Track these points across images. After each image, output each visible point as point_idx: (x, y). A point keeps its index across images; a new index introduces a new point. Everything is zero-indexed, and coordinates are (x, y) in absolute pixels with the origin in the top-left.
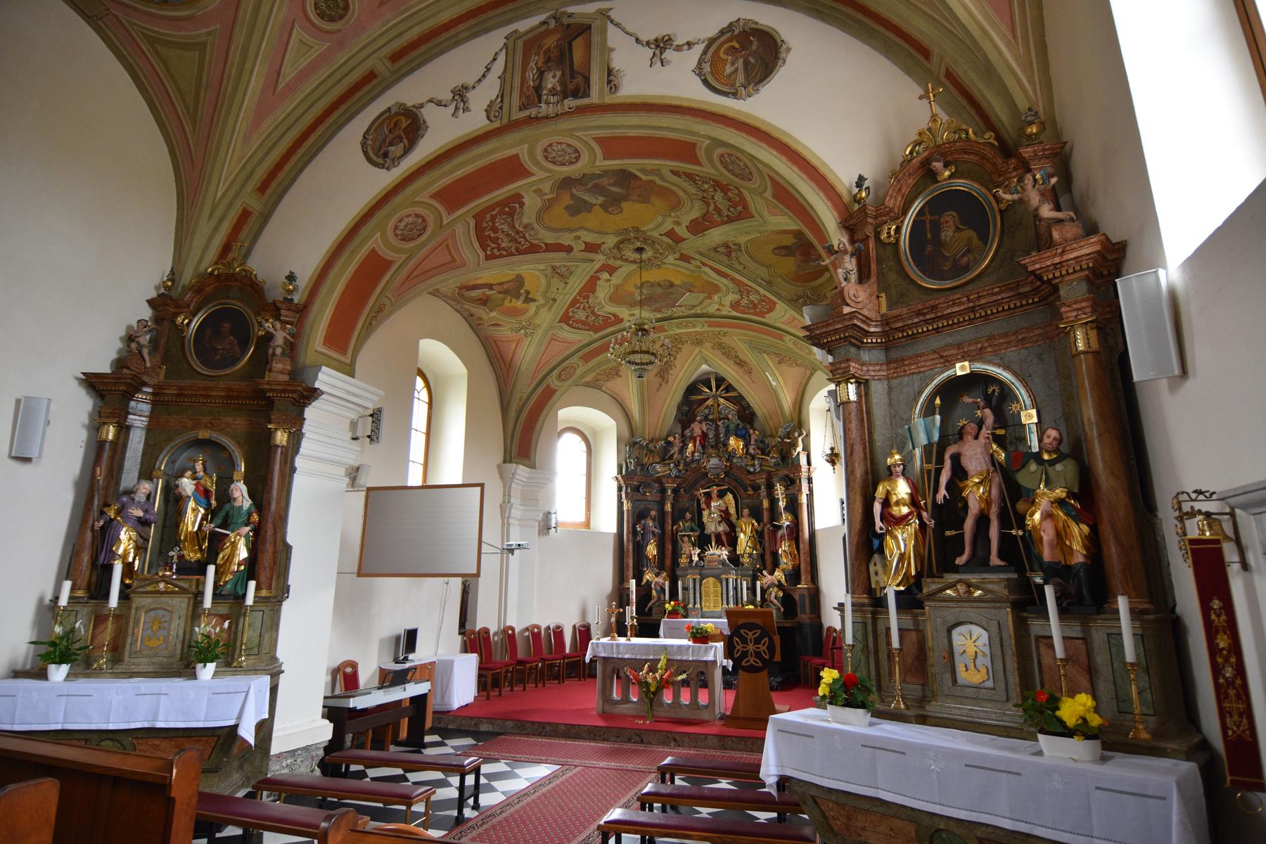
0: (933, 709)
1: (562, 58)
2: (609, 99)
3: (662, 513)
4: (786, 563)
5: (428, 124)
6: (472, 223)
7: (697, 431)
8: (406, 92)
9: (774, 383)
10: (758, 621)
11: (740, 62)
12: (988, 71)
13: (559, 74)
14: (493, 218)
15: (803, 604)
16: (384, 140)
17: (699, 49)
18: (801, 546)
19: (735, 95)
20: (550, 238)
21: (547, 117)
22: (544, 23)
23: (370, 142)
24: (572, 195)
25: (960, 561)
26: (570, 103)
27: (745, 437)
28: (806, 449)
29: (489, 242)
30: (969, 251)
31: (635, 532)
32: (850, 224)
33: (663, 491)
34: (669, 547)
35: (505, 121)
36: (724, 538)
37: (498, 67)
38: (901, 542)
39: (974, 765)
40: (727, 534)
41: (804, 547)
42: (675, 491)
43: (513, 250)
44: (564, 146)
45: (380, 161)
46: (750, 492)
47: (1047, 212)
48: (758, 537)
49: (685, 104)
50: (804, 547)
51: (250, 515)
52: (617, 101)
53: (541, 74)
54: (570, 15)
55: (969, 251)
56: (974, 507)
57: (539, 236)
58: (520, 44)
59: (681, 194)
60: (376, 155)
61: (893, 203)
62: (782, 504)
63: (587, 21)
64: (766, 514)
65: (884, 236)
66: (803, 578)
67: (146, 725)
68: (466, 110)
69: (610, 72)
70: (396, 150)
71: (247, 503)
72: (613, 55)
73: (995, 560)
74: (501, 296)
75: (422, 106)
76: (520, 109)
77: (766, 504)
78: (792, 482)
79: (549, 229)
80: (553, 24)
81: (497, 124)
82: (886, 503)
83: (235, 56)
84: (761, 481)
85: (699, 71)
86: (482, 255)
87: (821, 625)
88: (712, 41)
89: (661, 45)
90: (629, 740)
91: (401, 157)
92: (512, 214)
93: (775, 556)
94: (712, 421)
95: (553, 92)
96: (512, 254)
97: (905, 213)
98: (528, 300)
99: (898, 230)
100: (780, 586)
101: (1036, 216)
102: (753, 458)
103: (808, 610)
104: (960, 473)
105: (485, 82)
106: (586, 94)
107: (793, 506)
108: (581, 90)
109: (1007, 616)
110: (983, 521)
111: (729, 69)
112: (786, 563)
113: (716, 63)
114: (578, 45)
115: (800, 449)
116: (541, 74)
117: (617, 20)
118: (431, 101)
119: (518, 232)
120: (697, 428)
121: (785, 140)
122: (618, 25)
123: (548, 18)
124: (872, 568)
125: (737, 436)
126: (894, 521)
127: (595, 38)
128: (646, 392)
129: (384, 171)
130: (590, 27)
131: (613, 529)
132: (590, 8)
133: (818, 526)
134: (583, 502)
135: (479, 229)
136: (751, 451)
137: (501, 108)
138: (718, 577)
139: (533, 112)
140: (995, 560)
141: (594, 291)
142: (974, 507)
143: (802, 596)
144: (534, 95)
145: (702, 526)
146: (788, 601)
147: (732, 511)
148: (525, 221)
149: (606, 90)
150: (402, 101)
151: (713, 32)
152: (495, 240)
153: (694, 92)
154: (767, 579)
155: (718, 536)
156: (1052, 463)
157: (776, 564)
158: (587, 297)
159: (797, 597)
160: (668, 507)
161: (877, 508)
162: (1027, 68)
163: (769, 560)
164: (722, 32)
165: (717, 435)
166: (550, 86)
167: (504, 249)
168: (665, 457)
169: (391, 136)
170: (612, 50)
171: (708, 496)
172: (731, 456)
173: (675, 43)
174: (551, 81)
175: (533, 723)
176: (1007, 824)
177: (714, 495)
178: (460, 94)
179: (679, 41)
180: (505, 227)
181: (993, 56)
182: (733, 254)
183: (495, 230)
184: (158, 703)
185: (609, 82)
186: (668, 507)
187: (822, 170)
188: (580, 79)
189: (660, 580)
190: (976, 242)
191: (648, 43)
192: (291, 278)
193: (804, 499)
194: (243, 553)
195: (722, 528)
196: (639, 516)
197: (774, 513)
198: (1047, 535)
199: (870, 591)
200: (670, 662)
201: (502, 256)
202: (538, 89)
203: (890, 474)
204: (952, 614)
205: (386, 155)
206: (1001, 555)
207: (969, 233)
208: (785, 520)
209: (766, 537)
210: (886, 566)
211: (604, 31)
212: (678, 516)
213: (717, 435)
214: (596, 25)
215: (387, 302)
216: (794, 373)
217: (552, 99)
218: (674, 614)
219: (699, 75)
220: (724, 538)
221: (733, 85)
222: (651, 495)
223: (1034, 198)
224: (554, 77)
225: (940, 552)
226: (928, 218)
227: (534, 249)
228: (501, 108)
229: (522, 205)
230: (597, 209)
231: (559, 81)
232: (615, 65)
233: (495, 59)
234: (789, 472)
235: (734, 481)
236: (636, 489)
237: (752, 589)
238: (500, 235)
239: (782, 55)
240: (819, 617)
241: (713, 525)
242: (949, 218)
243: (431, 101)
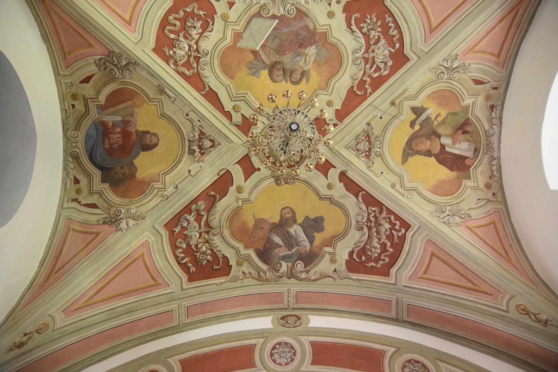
6: (393, 270)
14: (377, 260)
20: (351, 202)
24: (311, 243)
29: (396, 240)
43: (384, 214)
44: (278, 361)
57: (357, 210)
59: (227, 233)
74: (440, 131)
79: (346, 213)
86: (409, 235)
92: (363, 251)
96: (390, 211)
98: (417, 111)
119: (370, 228)
135: (394, 258)
141: (351, 91)
148: (358, 235)
152: (390, 237)
158: (362, 83)
167: (390, 223)
180: (375, 243)
182: (197, 134)
183: (384, 245)
201: (397, 217)
215: (512, 304)
227: (370, 200)
229: (351, 254)
230: (300, 220)
238: (384, 239)
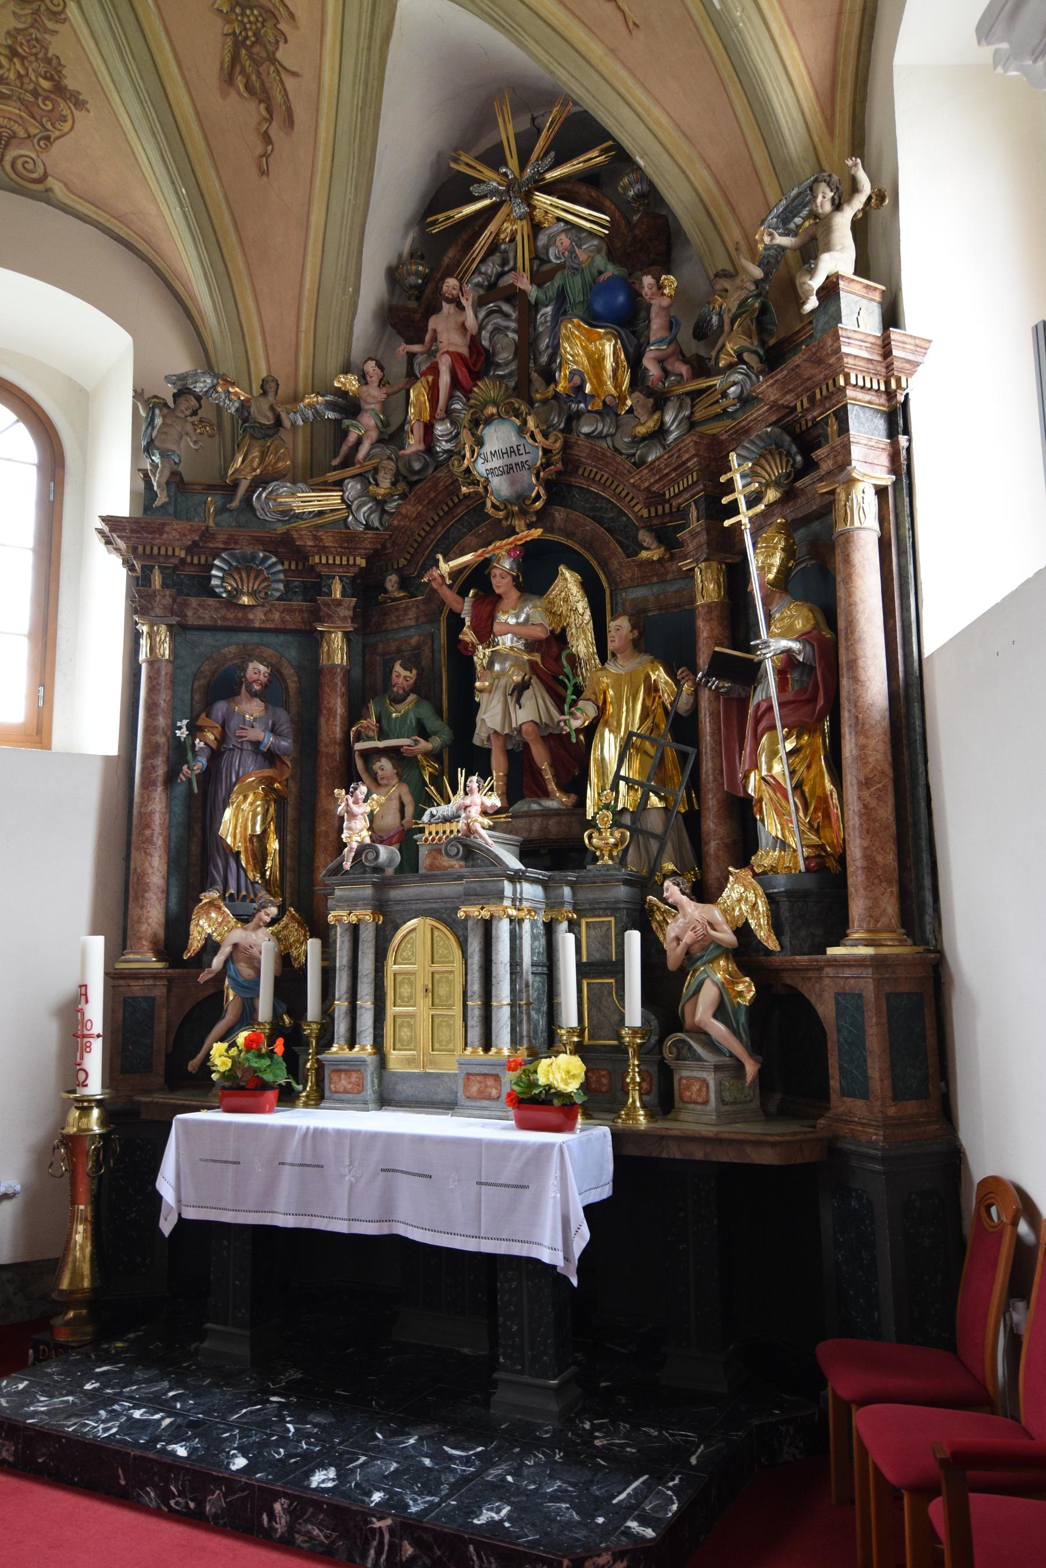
3: (314, 674)
15: (856, 1043)
27: (628, 321)
28: (876, 258)
36: (540, 756)
46: (652, 553)
50: (864, 746)
66: (857, 907)
78: (808, 444)
87: (953, 1159)
93: (743, 814)
100: (745, 951)
102: (659, 402)
103: (876, 1069)
115: (839, 259)
120: (448, 331)
125: (593, 319)
128: (212, 184)
131: (111, 747)
133: (938, 627)
134: (19, 653)
136: (649, 363)
138: (445, 915)
143: (850, 1004)
146: (783, 1025)
157: (744, 844)
159: (826, 1009)
163: (713, 833)
172: (568, 410)
177: (501, 582)
186: (336, 650)
208: (777, 641)
209: (706, 725)
218: (244, 1090)
235: (579, 519)
240: (945, 1110)
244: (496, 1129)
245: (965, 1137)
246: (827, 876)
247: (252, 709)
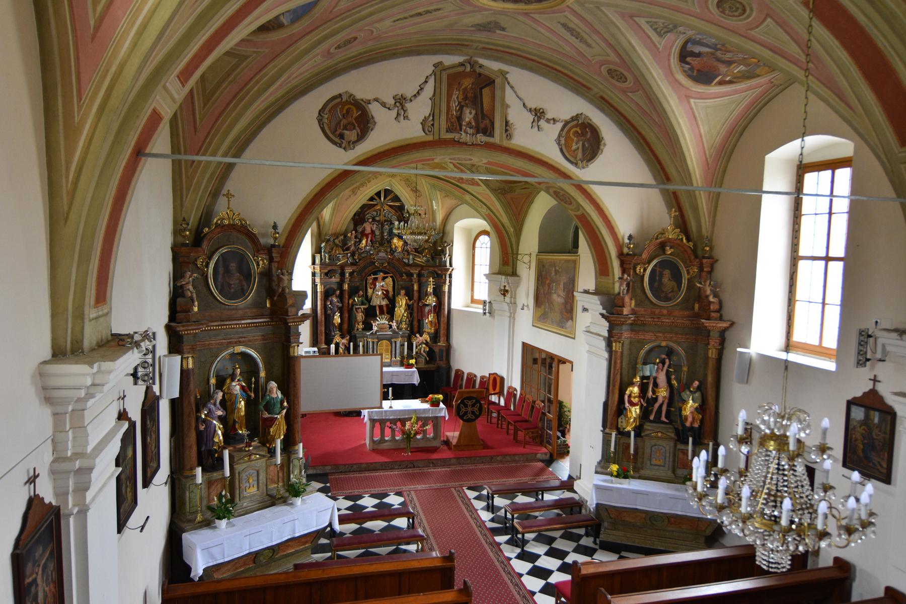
0: (642, 472)
1: (474, 99)
2: (505, 143)
3: (342, 291)
4: (428, 328)
5: (376, 120)
7: (368, 231)
8: (358, 84)
9: (435, 207)
10: (474, 395)
11: (581, 143)
12: (695, 209)
13: (474, 112)
16: (339, 123)
17: (559, 125)
18: (442, 319)
19: (576, 164)
21: (466, 144)
22: (462, 64)
23: (326, 121)
25: (652, 418)
26: (481, 138)
30: (672, 292)
31: (325, 307)
32: (621, 256)
33: (342, 275)
34: (346, 315)
35: (437, 137)
36: (385, 309)
37: (429, 89)
38: (635, 411)
39: (672, 497)
40: (387, 305)
41: (443, 320)
42: (351, 274)
45: (337, 140)
46: (405, 277)
47: (711, 299)
48: (409, 307)
49: (550, 162)
51: (282, 402)
52: (510, 146)
53: (461, 108)
54: (481, 66)
55: (672, 292)
56: (660, 400)
58: (445, 76)
60: (333, 133)
61: (645, 256)
62: (430, 289)
63: (492, 76)
64: (416, 295)
65: (638, 271)
66: (442, 339)
67: (289, 537)
68: (406, 118)
69: (507, 123)
70: (351, 135)
71: (280, 395)
72: (509, 111)
73: (663, 418)
75: (369, 102)
76: (447, 131)
77: (416, 287)
80: (468, 69)
81: (430, 138)
82: (630, 396)
83: (271, 70)
84: (415, 271)
85: (558, 141)
87: (449, 368)
88: (566, 123)
89: (539, 114)
90: (407, 467)
91: (355, 142)
94: (378, 221)
95: (469, 124)
97: (649, 263)
99: (645, 270)
100: (427, 344)
101: (707, 297)
102: (409, 254)
104: (656, 385)
105: (419, 98)
106: (491, 135)
107: (438, 293)
108: (488, 131)
109: (672, 444)
110: (661, 406)
111: (574, 147)
112: (428, 328)
113: (567, 138)
114: (486, 91)
116: (461, 108)
117: (512, 83)
118: (376, 100)
120: (368, 227)
121: (598, 201)
122: (512, 87)
123: (465, 61)
124: (620, 420)
126: (632, 404)
127: (498, 93)
129: (342, 150)
130: (494, 81)
132: (492, 66)
133: (453, 306)
137: (433, 125)
139: (456, 136)
140: (663, 418)
142: (660, 400)
144: (456, 124)
145: (369, 300)
146: (431, 353)
147: (390, 289)
149: (505, 136)
150: (354, 93)
151: (567, 117)
153: (554, 154)
154: (418, 339)
155: (381, 307)
156: (695, 392)
160: (346, 287)
161: (626, 397)
162: (709, 213)
164: (573, 119)
165: (382, 233)
166: (467, 120)
168: (344, 247)
169: (344, 122)
170: (508, 106)
171: (375, 279)
172: (392, 252)
173: (547, 116)
174: (468, 116)
175: (345, 465)
176: (680, 513)
178: (401, 102)
179: (549, 116)
181: (700, 206)
184: (294, 525)
185: (506, 131)
186: (346, 287)
187: (613, 224)
188: (487, 121)
189: (344, 341)
190: (676, 289)
191: (530, 110)
192: (275, 227)
193: (446, 289)
194: (283, 427)
195: (384, 303)
196: (327, 294)
197: (422, 294)
198: (690, 419)
199: (618, 429)
200: (418, 419)
202: (459, 119)
203: (632, 384)
204: (653, 442)
205: (342, 136)
206: (667, 417)
207: (674, 283)
210: (628, 422)
211: (503, 90)
212: (353, 291)
213: (382, 233)
214: (498, 81)
216: (450, 202)
217: (470, 131)
219: (559, 144)
220: (385, 309)
221: (576, 158)
222: (335, 279)
223: (708, 292)
224: (470, 113)
225: (645, 414)
226: (658, 269)
228: (433, 125)
231: (474, 118)
232: (510, 118)
233: (426, 82)
234: (438, 268)
236: (326, 274)
237: (410, 347)
239: (602, 147)
241: (378, 300)
242: (667, 273)
243: (376, 100)
244: (402, 369)
245: (452, 364)
246: (437, 332)
247: (335, 300)
